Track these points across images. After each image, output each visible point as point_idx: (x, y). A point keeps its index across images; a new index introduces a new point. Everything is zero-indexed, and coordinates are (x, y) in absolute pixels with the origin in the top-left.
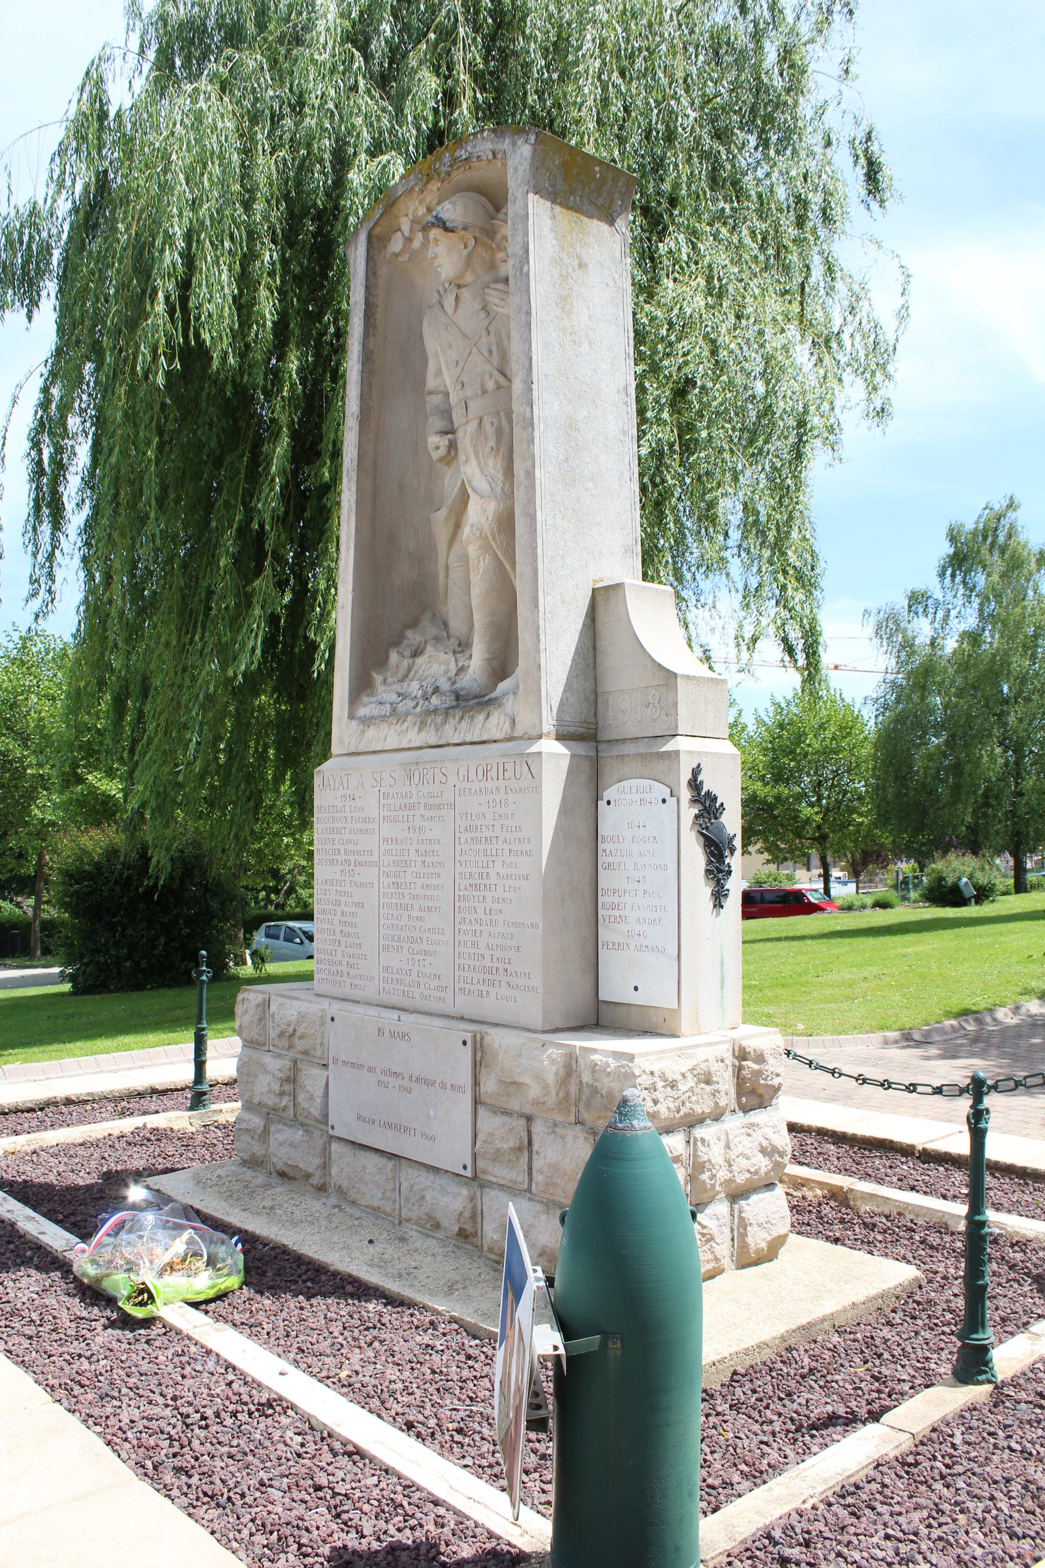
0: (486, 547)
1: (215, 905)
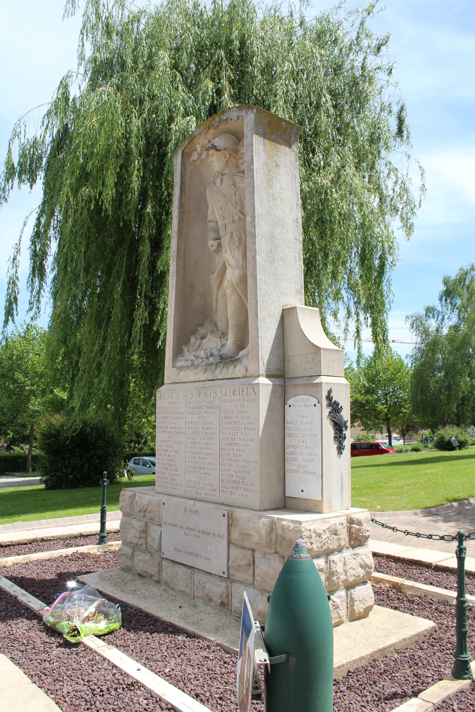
0: (234, 290)
1: (110, 450)
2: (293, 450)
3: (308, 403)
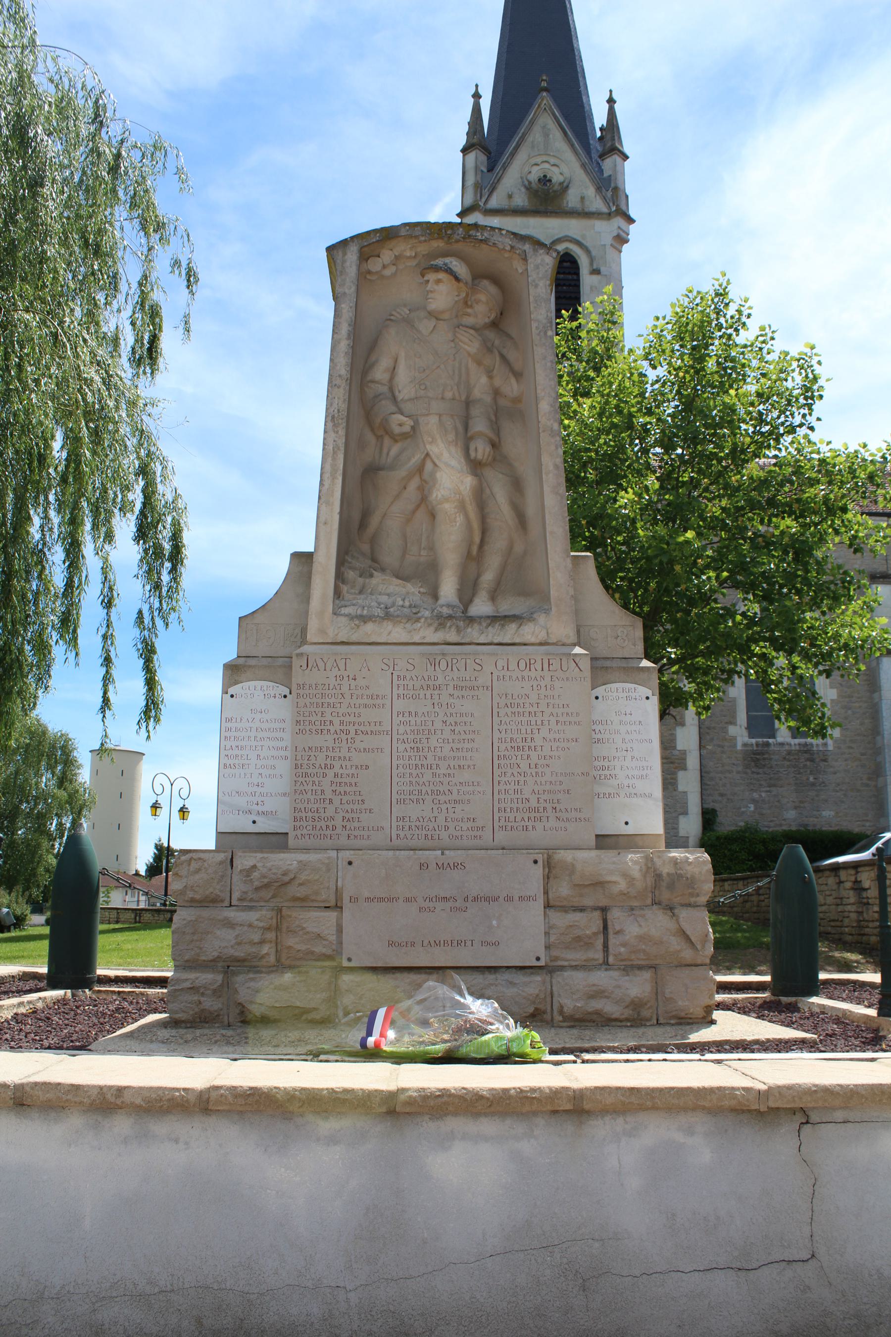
0: (462, 506)
1: (46, 780)
2: (606, 764)
3: (633, 695)
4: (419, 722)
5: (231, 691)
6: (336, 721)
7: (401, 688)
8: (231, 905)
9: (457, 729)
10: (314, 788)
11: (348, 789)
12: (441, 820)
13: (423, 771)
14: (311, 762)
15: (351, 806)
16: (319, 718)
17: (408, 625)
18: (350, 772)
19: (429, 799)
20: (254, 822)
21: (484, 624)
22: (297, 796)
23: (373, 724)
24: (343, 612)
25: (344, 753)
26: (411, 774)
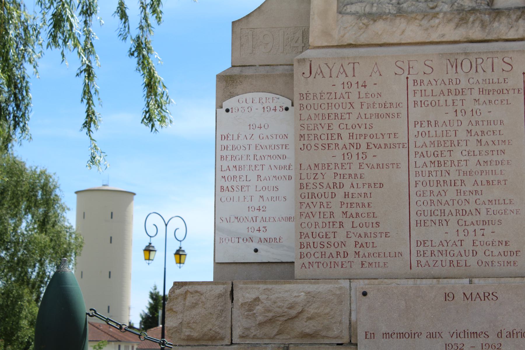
4: (439, 133)
5: (227, 104)
6: (345, 134)
7: (418, 94)
8: (232, 344)
9: (484, 139)
10: (322, 210)
11: (360, 210)
12: (468, 245)
13: (445, 188)
14: (318, 181)
15: (364, 229)
16: (325, 131)
17: (424, 22)
18: (363, 191)
19: (453, 220)
20: (256, 251)
21: (514, 17)
22: (303, 219)
23: (386, 136)
24: (348, 10)
25: (355, 169)
26: (431, 192)
